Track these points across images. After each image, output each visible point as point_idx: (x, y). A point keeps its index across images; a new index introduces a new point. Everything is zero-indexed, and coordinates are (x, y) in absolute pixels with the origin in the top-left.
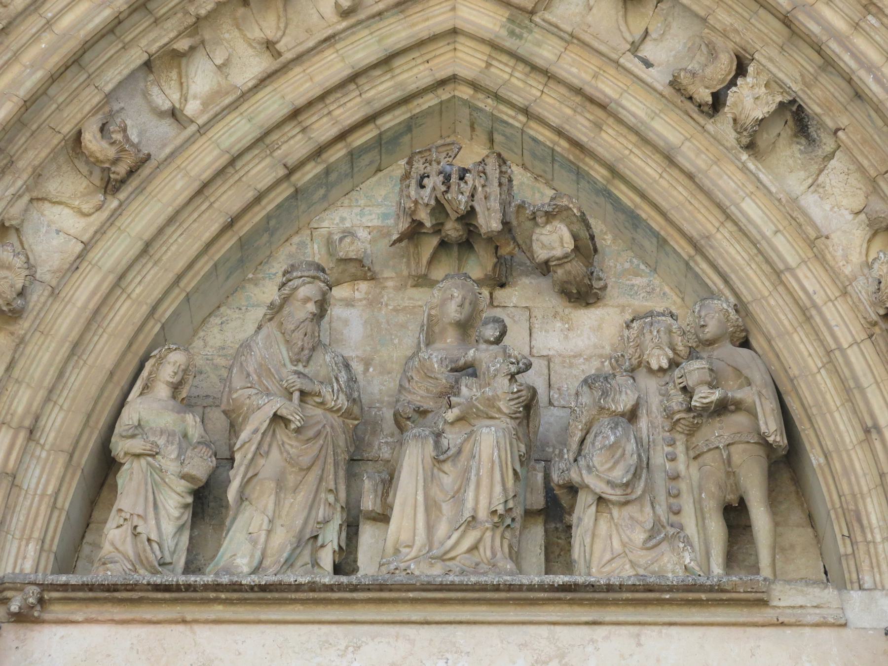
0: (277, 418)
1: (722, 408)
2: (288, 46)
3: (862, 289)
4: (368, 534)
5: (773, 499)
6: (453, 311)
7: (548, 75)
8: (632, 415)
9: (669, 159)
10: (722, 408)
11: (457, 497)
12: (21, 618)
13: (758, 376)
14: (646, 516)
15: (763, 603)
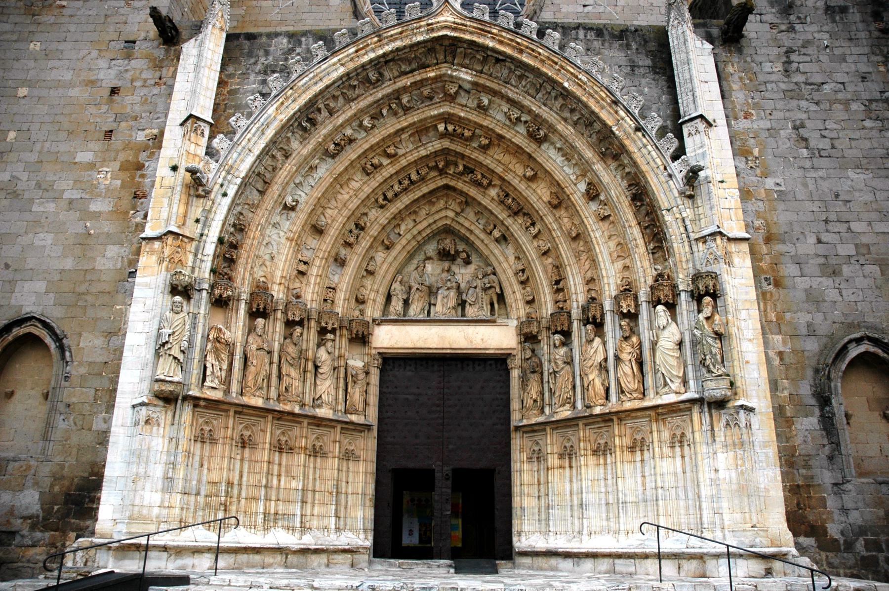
0: (418, 289)
1: (491, 287)
2: (418, 220)
3: (513, 267)
4: (432, 308)
5: (499, 303)
6: (446, 268)
7: (462, 225)
8: (475, 288)
9: (482, 241)
10: (491, 287)
11: (447, 303)
12: (379, 324)
13: (497, 281)
14: (477, 306)
15: (495, 322)
